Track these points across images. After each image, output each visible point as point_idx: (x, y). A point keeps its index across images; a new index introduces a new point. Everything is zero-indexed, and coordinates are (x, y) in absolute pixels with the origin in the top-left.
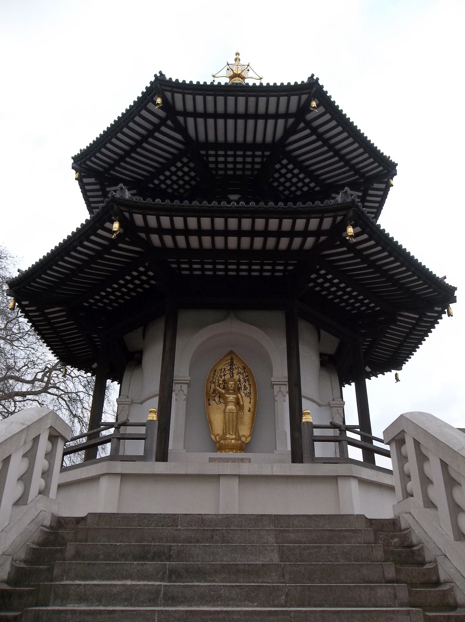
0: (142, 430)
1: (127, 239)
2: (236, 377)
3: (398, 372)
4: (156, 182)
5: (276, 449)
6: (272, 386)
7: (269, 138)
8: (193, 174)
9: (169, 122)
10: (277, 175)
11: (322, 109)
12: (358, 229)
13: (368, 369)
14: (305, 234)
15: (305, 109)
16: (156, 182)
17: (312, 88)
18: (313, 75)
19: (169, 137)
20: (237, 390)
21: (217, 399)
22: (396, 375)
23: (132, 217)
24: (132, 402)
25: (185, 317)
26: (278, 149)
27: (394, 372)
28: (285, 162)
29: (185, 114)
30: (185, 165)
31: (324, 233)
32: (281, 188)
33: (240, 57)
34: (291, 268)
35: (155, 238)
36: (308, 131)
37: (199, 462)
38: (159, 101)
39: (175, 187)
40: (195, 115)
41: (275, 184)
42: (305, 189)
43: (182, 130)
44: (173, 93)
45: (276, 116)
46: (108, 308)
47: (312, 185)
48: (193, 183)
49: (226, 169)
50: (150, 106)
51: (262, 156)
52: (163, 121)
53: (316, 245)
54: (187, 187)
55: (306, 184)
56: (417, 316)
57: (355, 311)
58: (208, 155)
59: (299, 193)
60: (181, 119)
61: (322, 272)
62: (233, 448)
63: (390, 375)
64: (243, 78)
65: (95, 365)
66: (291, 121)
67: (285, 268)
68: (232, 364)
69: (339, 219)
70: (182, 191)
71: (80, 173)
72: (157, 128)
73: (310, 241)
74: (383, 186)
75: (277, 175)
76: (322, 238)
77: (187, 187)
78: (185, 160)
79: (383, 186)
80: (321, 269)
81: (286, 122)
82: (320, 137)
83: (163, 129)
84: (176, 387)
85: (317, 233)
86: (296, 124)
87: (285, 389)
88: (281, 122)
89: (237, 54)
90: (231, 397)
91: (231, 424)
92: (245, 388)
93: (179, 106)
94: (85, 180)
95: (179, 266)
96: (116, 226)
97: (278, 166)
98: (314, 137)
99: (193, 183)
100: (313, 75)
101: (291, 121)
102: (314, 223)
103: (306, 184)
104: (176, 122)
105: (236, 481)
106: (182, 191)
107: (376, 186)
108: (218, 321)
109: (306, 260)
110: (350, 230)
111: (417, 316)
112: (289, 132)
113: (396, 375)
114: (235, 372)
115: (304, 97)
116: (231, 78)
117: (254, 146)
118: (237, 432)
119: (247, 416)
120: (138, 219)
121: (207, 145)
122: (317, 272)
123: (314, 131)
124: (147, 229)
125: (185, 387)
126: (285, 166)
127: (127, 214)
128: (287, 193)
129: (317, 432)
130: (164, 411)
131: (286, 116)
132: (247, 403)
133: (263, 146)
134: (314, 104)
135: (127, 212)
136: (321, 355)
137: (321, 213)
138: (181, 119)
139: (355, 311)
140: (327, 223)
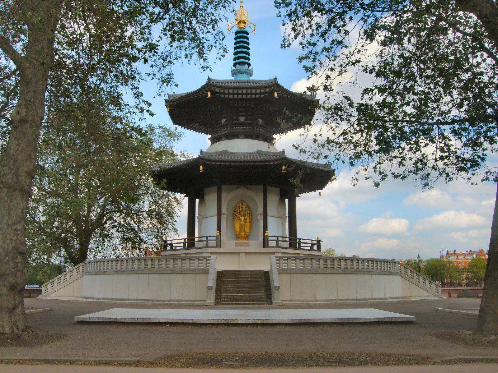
0: (215, 238)
2: (244, 209)
3: (321, 191)
20: (245, 215)
21: (237, 218)
25: (224, 187)
62: (243, 238)
63: (318, 192)
64: (245, 23)
68: (242, 204)
84: (222, 216)
87: (262, 217)
89: (241, 2)
90: (242, 218)
91: (243, 228)
92: (248, 214)
105: (244, 254)
108: (237, 188)
114: (244, 207)
118: (245, 232)
119: (248, 225)
125: (225, 216)
129: (270, 238)
132: (248, 220)
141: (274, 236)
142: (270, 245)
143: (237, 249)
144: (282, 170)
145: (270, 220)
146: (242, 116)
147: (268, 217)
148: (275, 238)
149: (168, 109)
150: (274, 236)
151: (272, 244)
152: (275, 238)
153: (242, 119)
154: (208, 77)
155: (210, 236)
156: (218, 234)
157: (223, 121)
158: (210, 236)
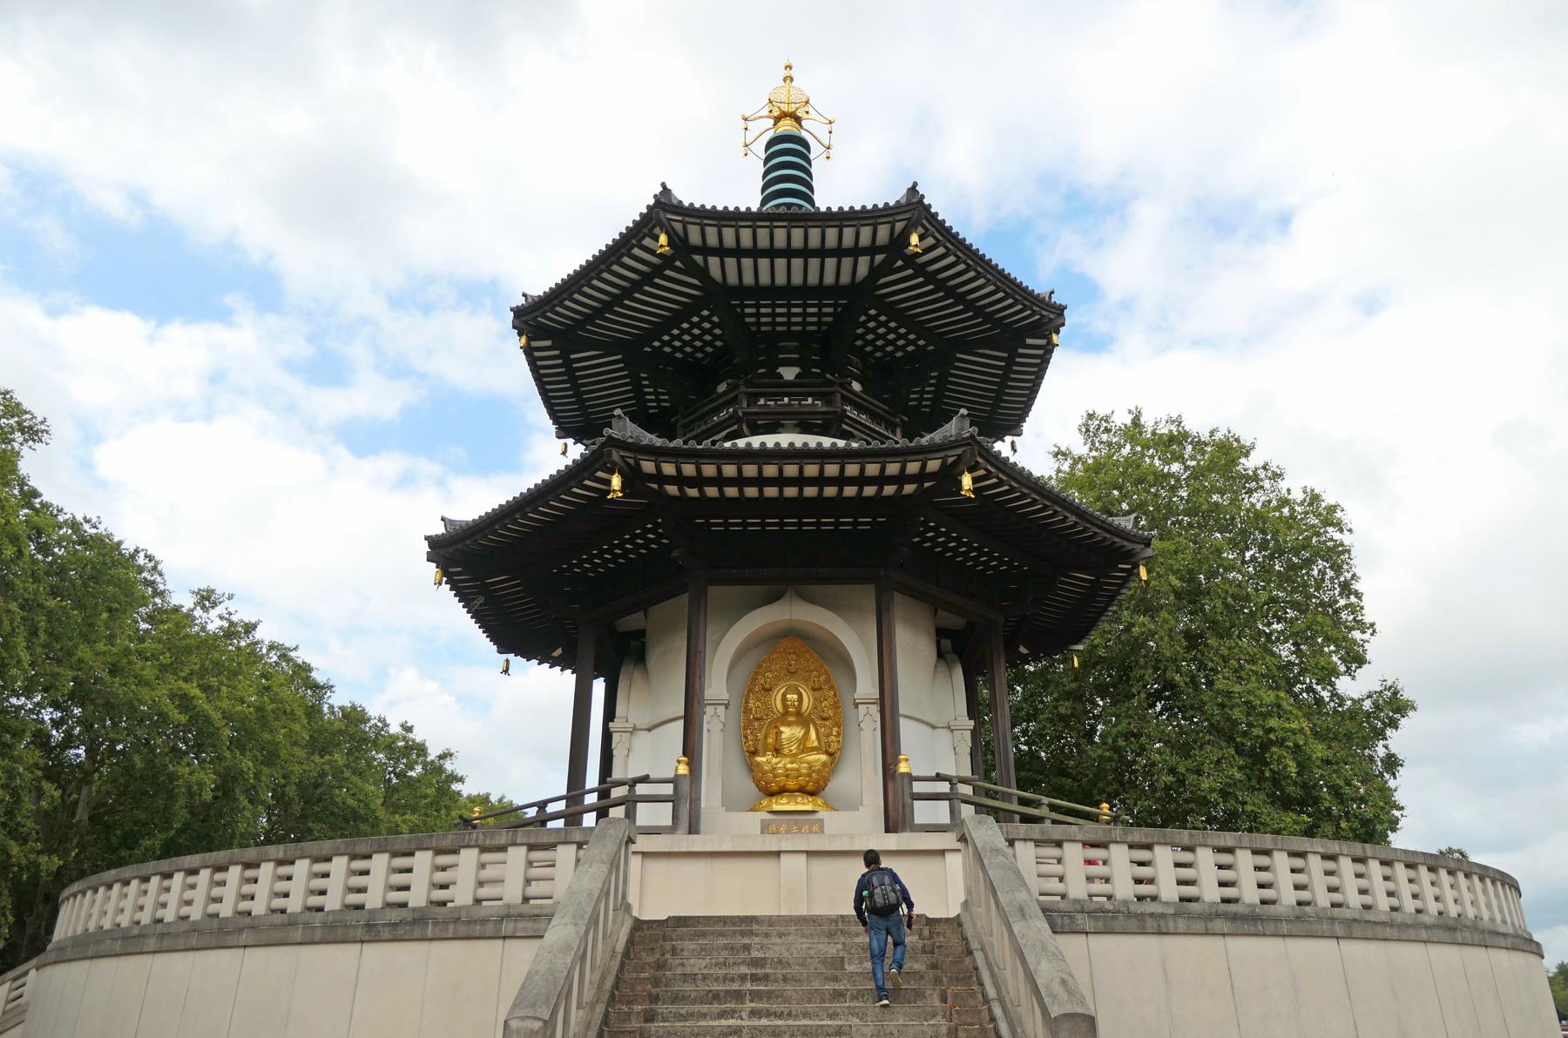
0: (668, 789)
4: (656, 344)
6: (856, 706)
7: (845, 279)
8: (717, 331)
9: (678, 263)
10: (860, 331)
11: (930, 241)
12: (982, 472)
13: (1023, 650)
14: (901, 479)
15: (900, 241)
16: (656, 344)
17: (914, 210)
18: (915, 184)
19: (680, 287)
24: (635, 729)
26: (857, 295)
28: (873, 312)
29: (706, 251)
30: (703, 319)
31: (932, 476)
32: (869, 349)
33: (792, 73)
35: (672, 490)
37: (745, 828)
38: (663, 239)
39: (688, 349)
40: (721, 252)
41: (859, 343)
42: (910, 348)
43: (703, 273)
45: (856, 252)
47: (921, 342)
48: (719, 343)
49: (774, 324)
50: (647, 242)
51: (835, 306)
53: (921, 492)
54: (709, 349)
55: (910, 342)
58: (744, 306)
59: (899, 354)
60: (698, 258)
64: (798, 120)
65: (558, 652)
66: (879, 258)
69: (950, 460)
70: (699, 355)
71: (529, 339)
72: (657, 270)
74: (1042, 342)
75: (860, 331)
76: (927, 485)
77: (709, 349)
78: (705, 313)
79: (1042, 342)
81: (872, 261)
85: (920, 477)
89: (789, 67)
94: (534, 344)
96: (616, 482)
97: (863, 318)
99: (719, 343)
100: (915, 184)
101: (879, 258)
102: (913, 467)
103: (910, 342)
105: (803, 857)
106: (699, 355)
107: (1029, 341)
110: (967, 481)
112: (875, 272)
115: (899, 226)
116: (777, 120)
117: (820, 291)
120: (648, 466)
121: (741, 291)
123: (920, 270)
124: (660, 478)
125: (721, 710)
126: (874, 318)
127: (631, 461)
128: (878, 354)
129: (918, 787)
130: (691, 749)
131: (872, 250)
133: (836, 290)
134: (914, 239)
136: (941, 633)
137: (924, 452)
138: (698, 258)
140: (933, 465)
141: (939, 777)
142: (919, 819)
143: (771, 844)
144: (960, 487)
145: (907, 729)
146: (788, 363)
147: (902, 721)
148: (944, 787)
149: (524, 339)
150: (939, 777)
151: (924, 812)
152: (944, 787)
153: (789, 373)
154: (663, 185)
155: (645, 779)
156: (683, 770)
157: (722, 388)
158: (645, 779)
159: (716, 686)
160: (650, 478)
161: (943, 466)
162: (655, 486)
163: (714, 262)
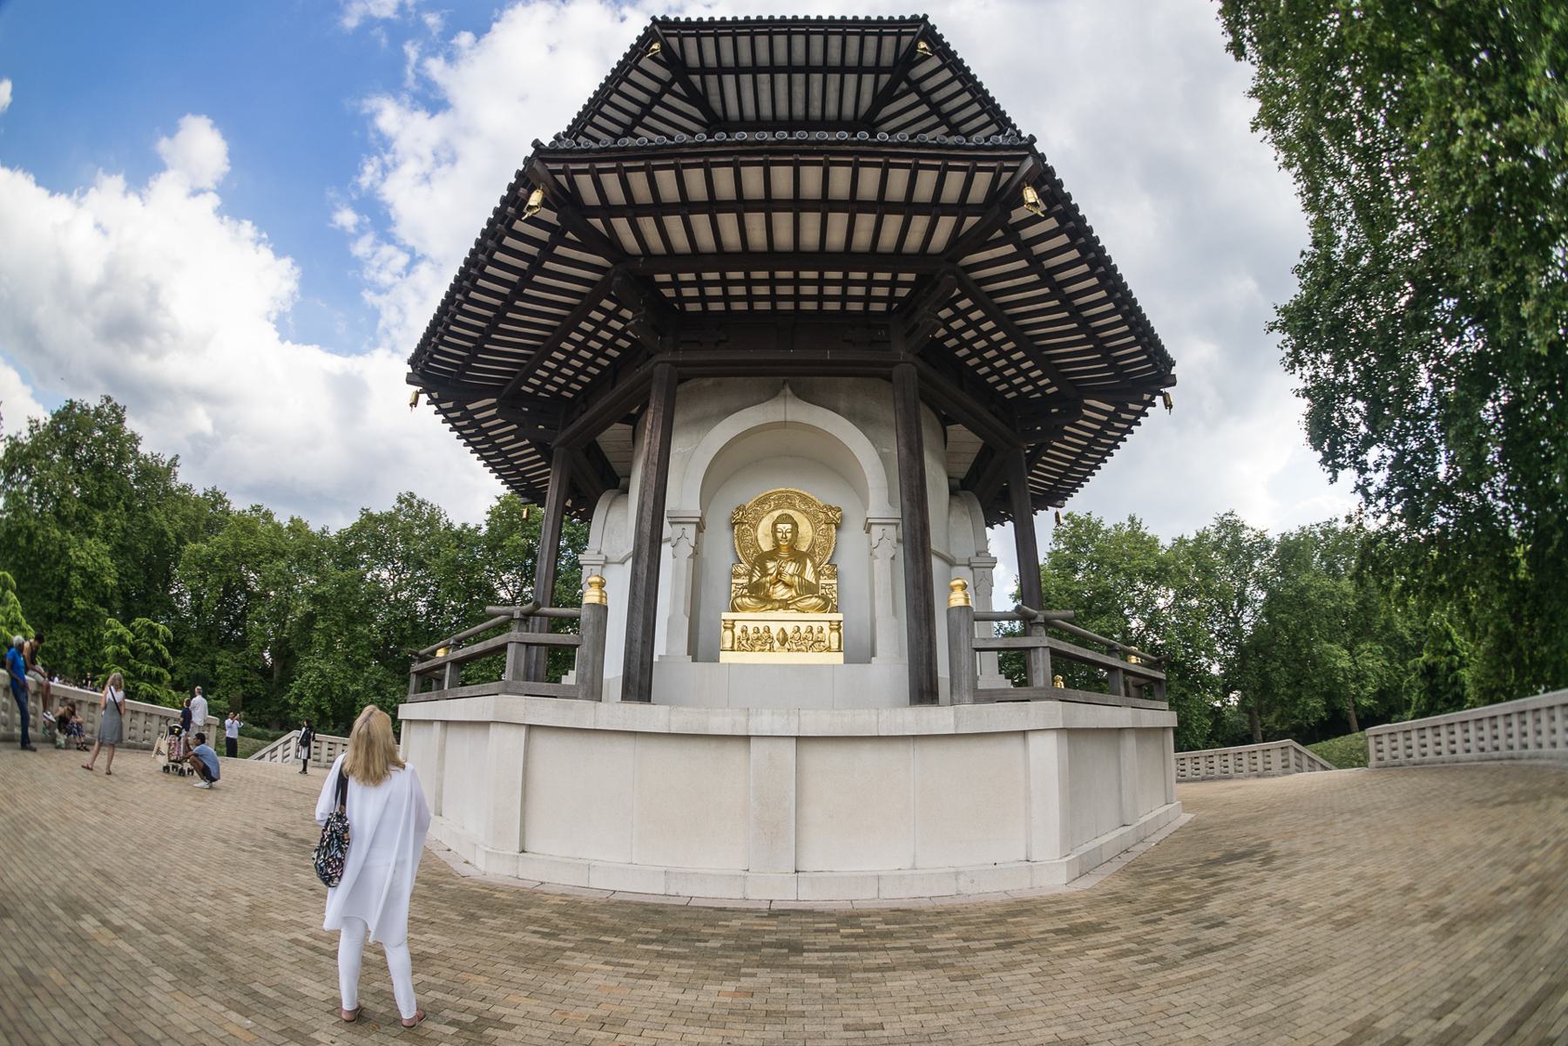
1: (570, 235)
5: (873, 655)
9: (676, 87)
22: (1057, 515)
23: (572, 182)
24: (607, 562)
27: (1052, 510)
29: (703, 70)
34: (902, 292)
36: (914, 97)
44: (681, 38)
46: (565, 393)
52: (666, 87)
56: (1112, 408)
57: (1013, 394)
61: (964, 304)
66: (885, 78)
67: (892, 292)
69: (1006, 176)
72: (656, 98)
73: (946, 224)
76: (971, 221)
80: (960, 298)
82: (935, 108)
83: (667, 98)
85: (961, 208)
86: (892, 85)
88: (868, 80)
93: (693, 58)
95: (678, 293)
98: (924, 109)
104: (688, 85)
109: (936, 274)
111: (1112, 408)
112: (883, 98)
113: (1057, 515)
122: (951, 304)
123: (925, 97)
124: (607, 210)
127: (562, 179)
131: (877, 70)
135: (560, 172)
138: (696, 79)
139: (1013, 394)
159: (683, 495)
160: (593, 211)
161: (995, 180)
162: (597, 222)
163: (712, 80)
